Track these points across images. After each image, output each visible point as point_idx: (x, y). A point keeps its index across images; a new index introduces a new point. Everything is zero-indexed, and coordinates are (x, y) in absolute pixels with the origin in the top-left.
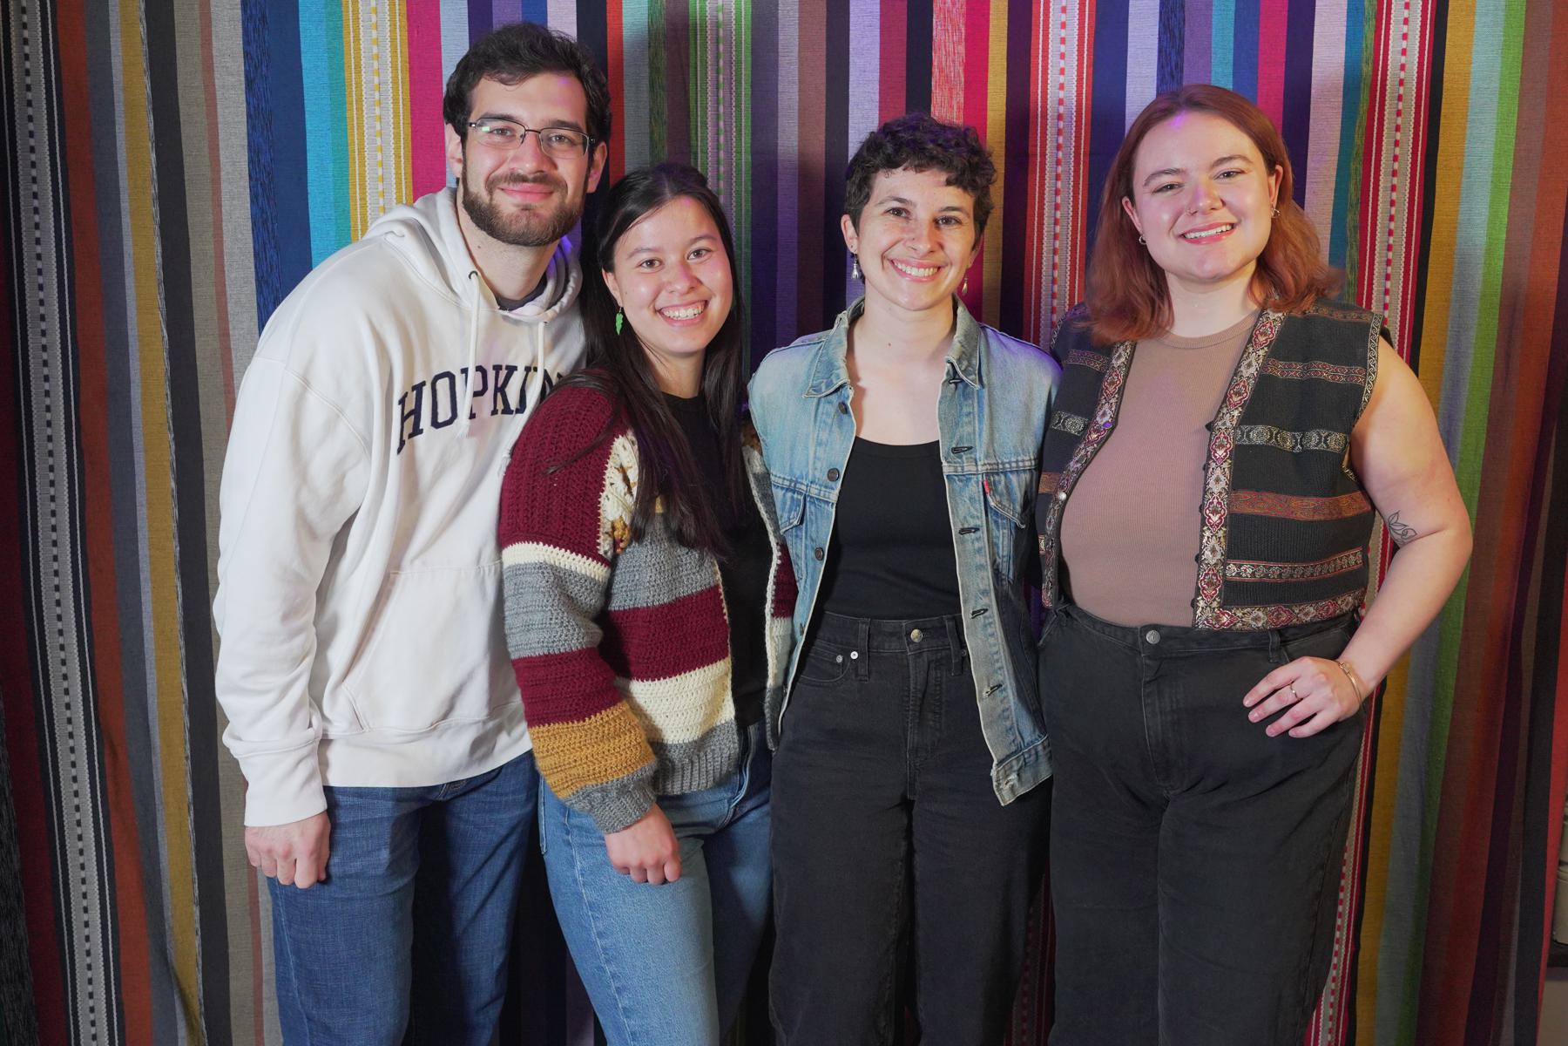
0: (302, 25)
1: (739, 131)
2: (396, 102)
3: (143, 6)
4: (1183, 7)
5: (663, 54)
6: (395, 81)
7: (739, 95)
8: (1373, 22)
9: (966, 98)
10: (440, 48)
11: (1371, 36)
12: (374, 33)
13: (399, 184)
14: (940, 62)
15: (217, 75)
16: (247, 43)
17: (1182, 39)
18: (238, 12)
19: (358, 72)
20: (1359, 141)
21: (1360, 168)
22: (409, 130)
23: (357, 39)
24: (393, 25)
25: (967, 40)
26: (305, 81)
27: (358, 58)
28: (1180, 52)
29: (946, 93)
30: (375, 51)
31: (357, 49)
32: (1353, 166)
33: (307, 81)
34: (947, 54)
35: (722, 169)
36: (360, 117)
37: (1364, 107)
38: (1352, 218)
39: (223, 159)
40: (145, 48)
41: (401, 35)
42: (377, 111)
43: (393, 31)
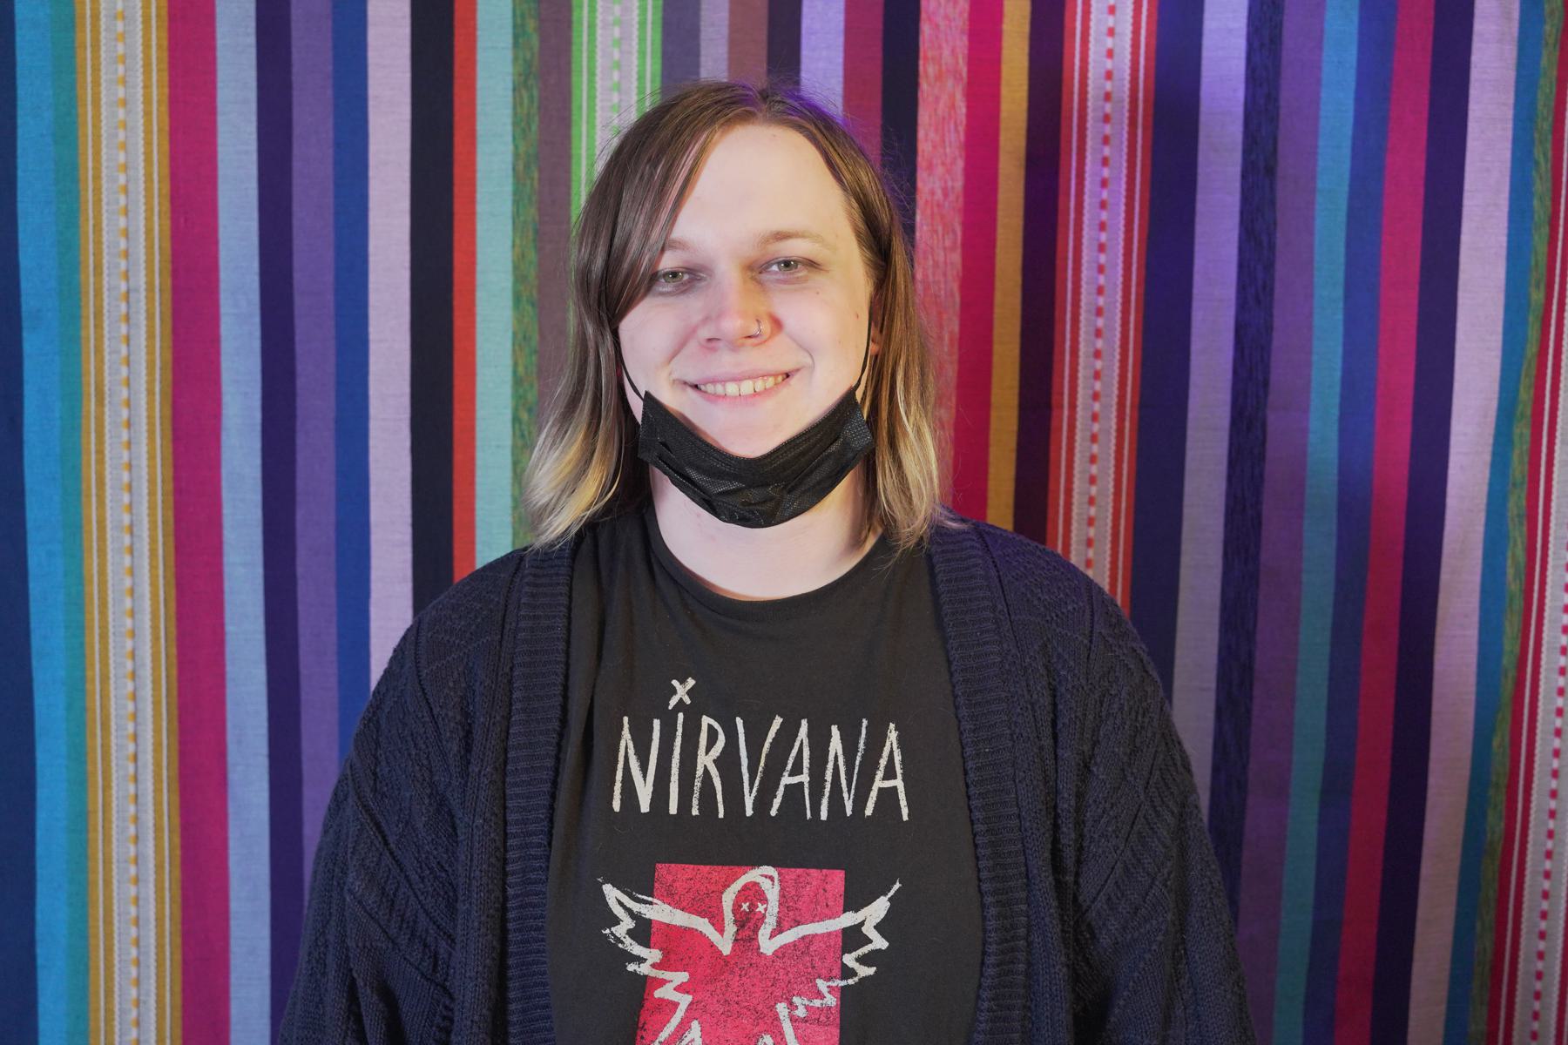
0: (20, 207)
2: (150, 317)
4: (1273, 203)
5: (532, 256)
8: (1545, 230)
9: (963, 325)
10: (215, 243)
11: (1542, 249)
12: (122, 222)
13: (151, 432)
14: (925, 276)
17: (1272, 247)
20: (1525, 395)
21: (1527, 432)
22: (169, 356)
24: (149, 210)
25: (963, 245)
26: (24, 285)
28: (1269, 267)
31: (98, 243)
32: (1517, 431)
34: (936, 264)
36: (99, 339)
37: (1532, 349)
38: (1516, 503)
41: (161, 225)
43: (149, 219)
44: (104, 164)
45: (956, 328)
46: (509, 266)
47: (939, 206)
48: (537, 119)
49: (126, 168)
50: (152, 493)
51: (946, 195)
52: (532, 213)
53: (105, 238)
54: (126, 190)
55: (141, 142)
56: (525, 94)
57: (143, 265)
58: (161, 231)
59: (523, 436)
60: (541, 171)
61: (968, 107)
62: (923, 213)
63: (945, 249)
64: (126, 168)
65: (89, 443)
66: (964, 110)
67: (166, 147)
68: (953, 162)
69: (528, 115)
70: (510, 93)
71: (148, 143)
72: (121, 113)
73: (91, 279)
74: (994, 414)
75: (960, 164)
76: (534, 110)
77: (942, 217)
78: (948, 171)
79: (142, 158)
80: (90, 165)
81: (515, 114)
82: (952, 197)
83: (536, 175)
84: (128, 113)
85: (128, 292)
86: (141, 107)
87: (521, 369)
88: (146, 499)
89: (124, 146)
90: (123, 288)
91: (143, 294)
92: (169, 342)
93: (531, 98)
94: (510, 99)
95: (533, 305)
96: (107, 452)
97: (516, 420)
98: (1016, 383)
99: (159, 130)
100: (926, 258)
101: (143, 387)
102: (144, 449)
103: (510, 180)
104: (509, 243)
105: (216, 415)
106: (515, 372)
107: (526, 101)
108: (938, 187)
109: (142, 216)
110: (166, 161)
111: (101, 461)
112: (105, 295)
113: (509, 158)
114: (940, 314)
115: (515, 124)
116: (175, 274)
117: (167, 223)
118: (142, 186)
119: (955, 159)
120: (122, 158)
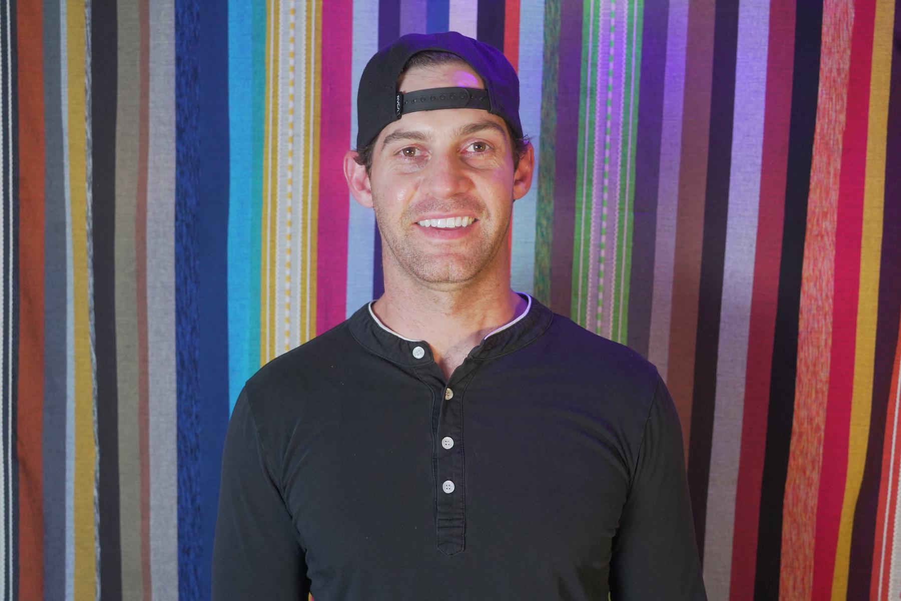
1: (623, 190)
3: (89, 60)
5: (554, 115)
6: (307, 134)
7: (624, 155)
12: (291, 90)
13: (304, 228)
14: (822, 129)
15: (151, 125)
16: (179, 94)
18: (172, 68)
19: (275, 124)
22: (317, 179)
23: (275, 95)
27: (275, 111)
29: (825, 159)
30: (291, 105)
31: (275, 104)
33: (234, 132)
34: (830, 121)
35: (604, 224)
36: (274, 167)
39: (150, 199)
40: (89, 97)
41: (315, 92)
42: (290, 161)
43: (307, 88)
44: (281, 52)
45: (839, 167)
46: (539, 122)
47: (834, 81)
48: (559, 23)
49: (294, 54)
50: (304, 269)
51: (839, 74)
52: (555, 86)
53: (280, 101)
54: (293, 69)
55: (304, 37)
56: (552, 4)
57: (303, 119)
58: (315, 96)
59: (543, 235)
60: (561, 57)
61: (856, 13)
62: (824, 85)
63: (836, 111)
64: (294, 54)
65: (266, 235)
66: (853, 15)
67: (320, 41)
68: (844, 52)
69: (554, 20)
70: (543, 5)
71: (308, 38)
72: (292, 18)
73: (271, 128)
74: (865, 227)
75: (849, 52)
76: (559, 17)
77: (836, 90)
78: (841, 58)
79: (304, 47)
80: (272, 52)
81: (546, 19)
82: (843, 76)
83: (557, 61)
84: (296, 18)
85: (293, 136)
86: (304, 14)
87: (543, 190)
88: (300, 272)
89: (293, 40)
90: (290, 133)
91: (303, 137)
92: (318, 170)
93: (556, 8)
94: (542, 9)
95: (553, 148)
96: (277, 241)
97: (538, 224)
98: (882, 205)
99: (316, 29)
100: (824, 117)
101: (300, 199)
102: (300, 240)
103: (541, 63)
104: (539, 106)
105: (346, 219)
106: (539, 193)
107: (553, 10)
108: (835, 67)
109: (303, 86)
110: (319, 50)
111: (273, 248)
112: (279, 137)
113: (541, 49)
114: (829, 157)
115: (545, 26)
116: (323, 124)
117: (319, 90)
118: (304, 66)
119: (845, 49)
120: (291, 47)
